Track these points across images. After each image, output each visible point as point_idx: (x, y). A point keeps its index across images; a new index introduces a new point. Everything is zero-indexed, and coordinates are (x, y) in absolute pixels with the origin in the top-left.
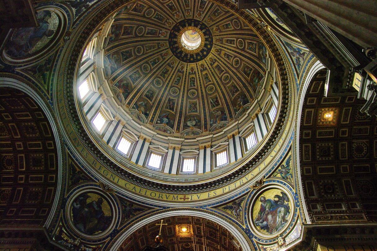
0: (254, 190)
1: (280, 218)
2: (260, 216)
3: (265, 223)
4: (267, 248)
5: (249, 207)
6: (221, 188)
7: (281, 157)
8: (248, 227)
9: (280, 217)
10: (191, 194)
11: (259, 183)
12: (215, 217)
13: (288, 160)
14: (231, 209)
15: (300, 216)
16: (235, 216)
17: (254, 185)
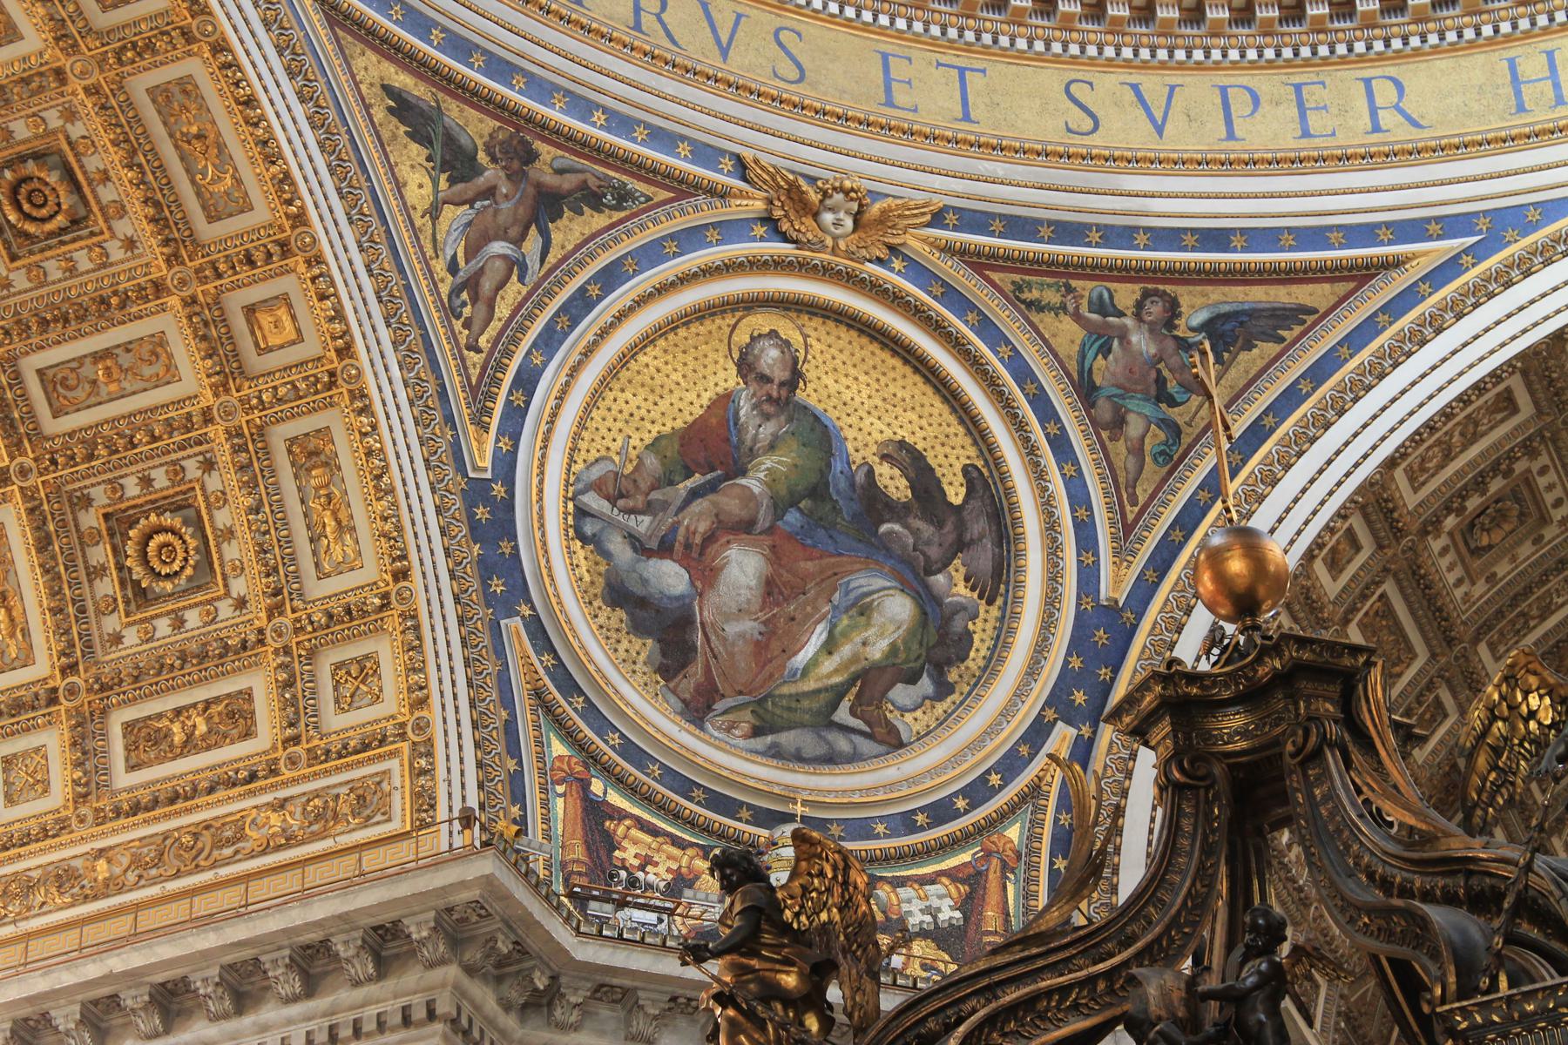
0: (768, 220)
3: (670, 577)
4: (622, 815)
5: (621, 317)
7: (1216, 239)
8: (510, 483)
9: (846, 650)
11: (857, 218)
13: (1254, 313)
14: (445, 166)
17: (814, 197)
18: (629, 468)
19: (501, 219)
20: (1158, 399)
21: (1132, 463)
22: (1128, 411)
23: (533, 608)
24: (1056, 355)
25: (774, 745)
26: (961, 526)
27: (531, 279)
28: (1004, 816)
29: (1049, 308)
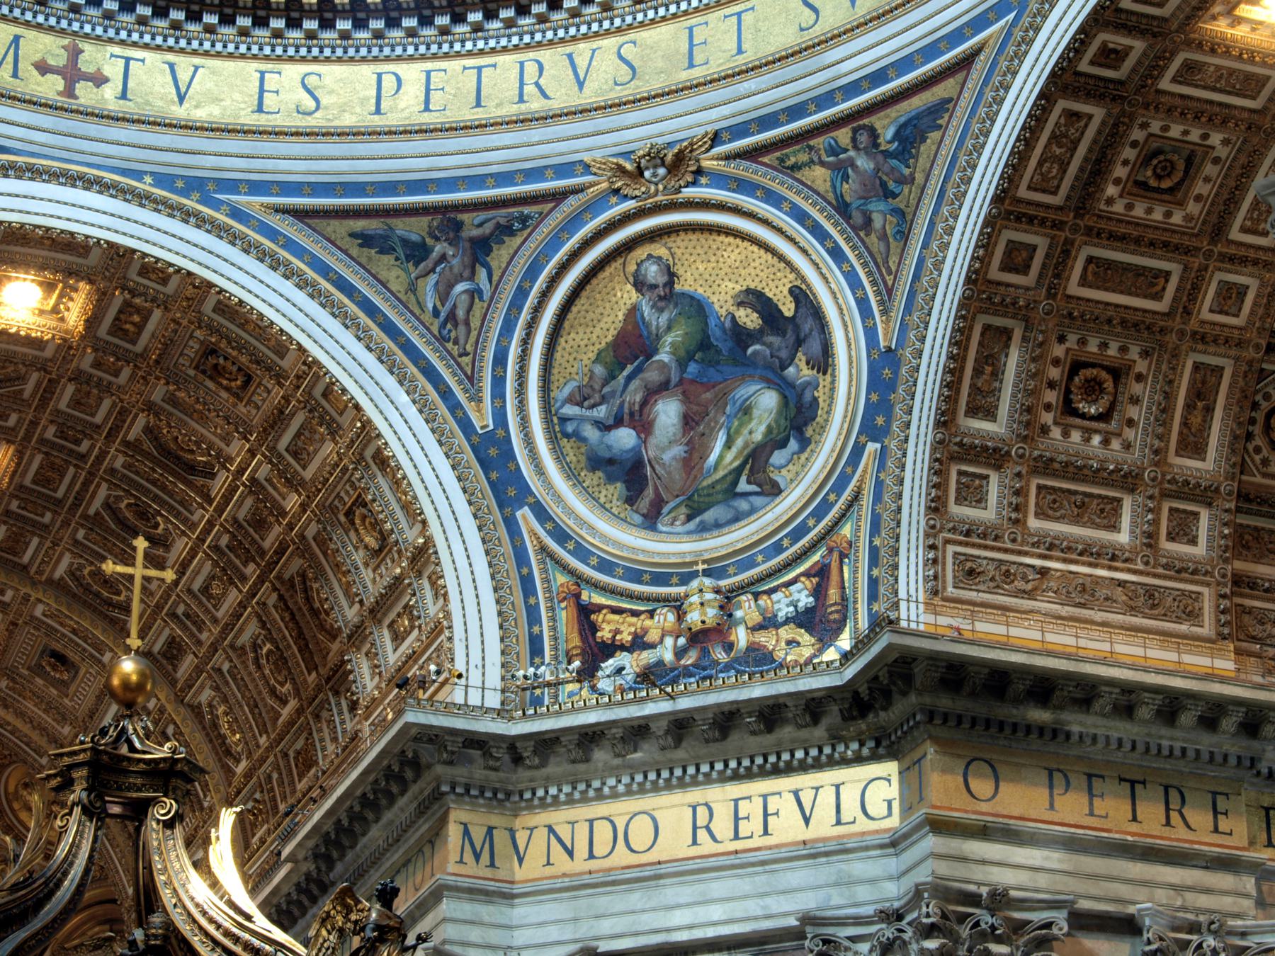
0: (616, 192)
1: (734, 450)
2: (606, 382)
3: (625, 438)
4: (599, 608)
6: (364, 60)
7: (879, 77)
9: (739, 442)
10: (122, 43)
11: (663, 164)
12: (288, 287)
13: (918, 117)
14: (408, 259)
15: (864, 503)
16: (427, 318)
17: (629, 166)
18: (586, 379)
19: (456, 270)
20: (886, 197)
21: (882, 248)
22: (871, 212)
23: (535, 497)
24: (818, 194)
25: (702, 522)
26: (797, 328)
27: (486, 296)
28: (837, 523)
29: (804, 165)
